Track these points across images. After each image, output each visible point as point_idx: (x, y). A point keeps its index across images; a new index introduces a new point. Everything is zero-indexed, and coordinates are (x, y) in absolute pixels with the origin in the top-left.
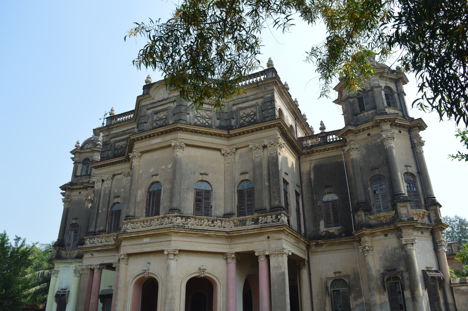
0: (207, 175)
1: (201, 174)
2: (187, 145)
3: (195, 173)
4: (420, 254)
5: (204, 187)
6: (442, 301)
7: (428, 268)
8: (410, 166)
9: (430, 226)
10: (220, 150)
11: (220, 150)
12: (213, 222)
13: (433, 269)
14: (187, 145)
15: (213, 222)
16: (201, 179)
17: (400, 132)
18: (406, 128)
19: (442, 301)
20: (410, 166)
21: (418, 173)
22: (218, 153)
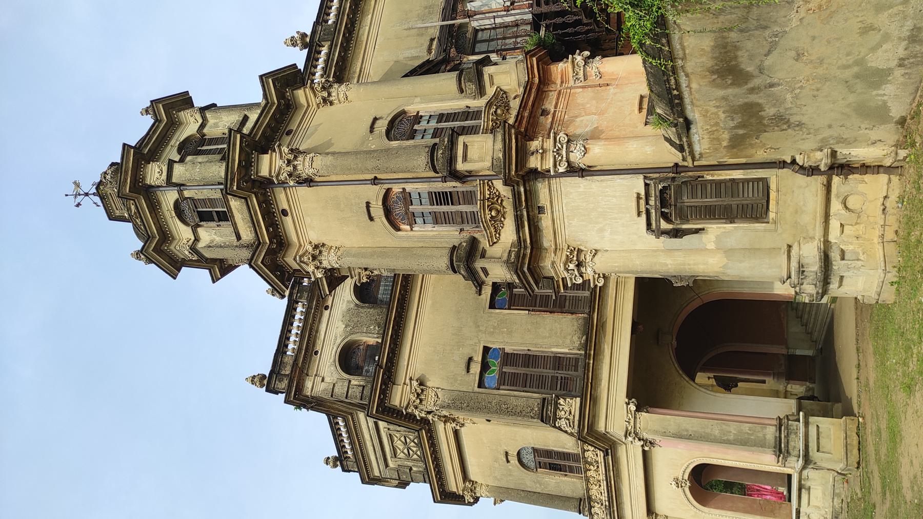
0: (507, 453)
1: (508, 461)
2: (465, 477)
3: (510, 470)
4: (601, 230)
5: (528, 458)
6: (737, 174)
7: (639, 214)
8: (368, 204)
9: (519, 193)
10: (456, 433)
11: (456, 433)
12: (591, 464)
13: (643, 193)
14: (465, 477)
15: (591, 464)
16: (517, 462)
17: (285, 213)
18: (265, 194)
19: (737, 174)
20: (368, 204)
21: (375, 181)
22: (464, 432)
